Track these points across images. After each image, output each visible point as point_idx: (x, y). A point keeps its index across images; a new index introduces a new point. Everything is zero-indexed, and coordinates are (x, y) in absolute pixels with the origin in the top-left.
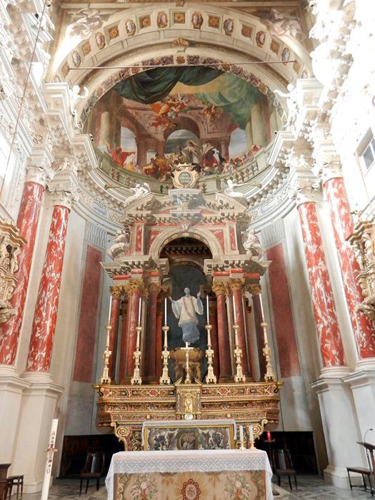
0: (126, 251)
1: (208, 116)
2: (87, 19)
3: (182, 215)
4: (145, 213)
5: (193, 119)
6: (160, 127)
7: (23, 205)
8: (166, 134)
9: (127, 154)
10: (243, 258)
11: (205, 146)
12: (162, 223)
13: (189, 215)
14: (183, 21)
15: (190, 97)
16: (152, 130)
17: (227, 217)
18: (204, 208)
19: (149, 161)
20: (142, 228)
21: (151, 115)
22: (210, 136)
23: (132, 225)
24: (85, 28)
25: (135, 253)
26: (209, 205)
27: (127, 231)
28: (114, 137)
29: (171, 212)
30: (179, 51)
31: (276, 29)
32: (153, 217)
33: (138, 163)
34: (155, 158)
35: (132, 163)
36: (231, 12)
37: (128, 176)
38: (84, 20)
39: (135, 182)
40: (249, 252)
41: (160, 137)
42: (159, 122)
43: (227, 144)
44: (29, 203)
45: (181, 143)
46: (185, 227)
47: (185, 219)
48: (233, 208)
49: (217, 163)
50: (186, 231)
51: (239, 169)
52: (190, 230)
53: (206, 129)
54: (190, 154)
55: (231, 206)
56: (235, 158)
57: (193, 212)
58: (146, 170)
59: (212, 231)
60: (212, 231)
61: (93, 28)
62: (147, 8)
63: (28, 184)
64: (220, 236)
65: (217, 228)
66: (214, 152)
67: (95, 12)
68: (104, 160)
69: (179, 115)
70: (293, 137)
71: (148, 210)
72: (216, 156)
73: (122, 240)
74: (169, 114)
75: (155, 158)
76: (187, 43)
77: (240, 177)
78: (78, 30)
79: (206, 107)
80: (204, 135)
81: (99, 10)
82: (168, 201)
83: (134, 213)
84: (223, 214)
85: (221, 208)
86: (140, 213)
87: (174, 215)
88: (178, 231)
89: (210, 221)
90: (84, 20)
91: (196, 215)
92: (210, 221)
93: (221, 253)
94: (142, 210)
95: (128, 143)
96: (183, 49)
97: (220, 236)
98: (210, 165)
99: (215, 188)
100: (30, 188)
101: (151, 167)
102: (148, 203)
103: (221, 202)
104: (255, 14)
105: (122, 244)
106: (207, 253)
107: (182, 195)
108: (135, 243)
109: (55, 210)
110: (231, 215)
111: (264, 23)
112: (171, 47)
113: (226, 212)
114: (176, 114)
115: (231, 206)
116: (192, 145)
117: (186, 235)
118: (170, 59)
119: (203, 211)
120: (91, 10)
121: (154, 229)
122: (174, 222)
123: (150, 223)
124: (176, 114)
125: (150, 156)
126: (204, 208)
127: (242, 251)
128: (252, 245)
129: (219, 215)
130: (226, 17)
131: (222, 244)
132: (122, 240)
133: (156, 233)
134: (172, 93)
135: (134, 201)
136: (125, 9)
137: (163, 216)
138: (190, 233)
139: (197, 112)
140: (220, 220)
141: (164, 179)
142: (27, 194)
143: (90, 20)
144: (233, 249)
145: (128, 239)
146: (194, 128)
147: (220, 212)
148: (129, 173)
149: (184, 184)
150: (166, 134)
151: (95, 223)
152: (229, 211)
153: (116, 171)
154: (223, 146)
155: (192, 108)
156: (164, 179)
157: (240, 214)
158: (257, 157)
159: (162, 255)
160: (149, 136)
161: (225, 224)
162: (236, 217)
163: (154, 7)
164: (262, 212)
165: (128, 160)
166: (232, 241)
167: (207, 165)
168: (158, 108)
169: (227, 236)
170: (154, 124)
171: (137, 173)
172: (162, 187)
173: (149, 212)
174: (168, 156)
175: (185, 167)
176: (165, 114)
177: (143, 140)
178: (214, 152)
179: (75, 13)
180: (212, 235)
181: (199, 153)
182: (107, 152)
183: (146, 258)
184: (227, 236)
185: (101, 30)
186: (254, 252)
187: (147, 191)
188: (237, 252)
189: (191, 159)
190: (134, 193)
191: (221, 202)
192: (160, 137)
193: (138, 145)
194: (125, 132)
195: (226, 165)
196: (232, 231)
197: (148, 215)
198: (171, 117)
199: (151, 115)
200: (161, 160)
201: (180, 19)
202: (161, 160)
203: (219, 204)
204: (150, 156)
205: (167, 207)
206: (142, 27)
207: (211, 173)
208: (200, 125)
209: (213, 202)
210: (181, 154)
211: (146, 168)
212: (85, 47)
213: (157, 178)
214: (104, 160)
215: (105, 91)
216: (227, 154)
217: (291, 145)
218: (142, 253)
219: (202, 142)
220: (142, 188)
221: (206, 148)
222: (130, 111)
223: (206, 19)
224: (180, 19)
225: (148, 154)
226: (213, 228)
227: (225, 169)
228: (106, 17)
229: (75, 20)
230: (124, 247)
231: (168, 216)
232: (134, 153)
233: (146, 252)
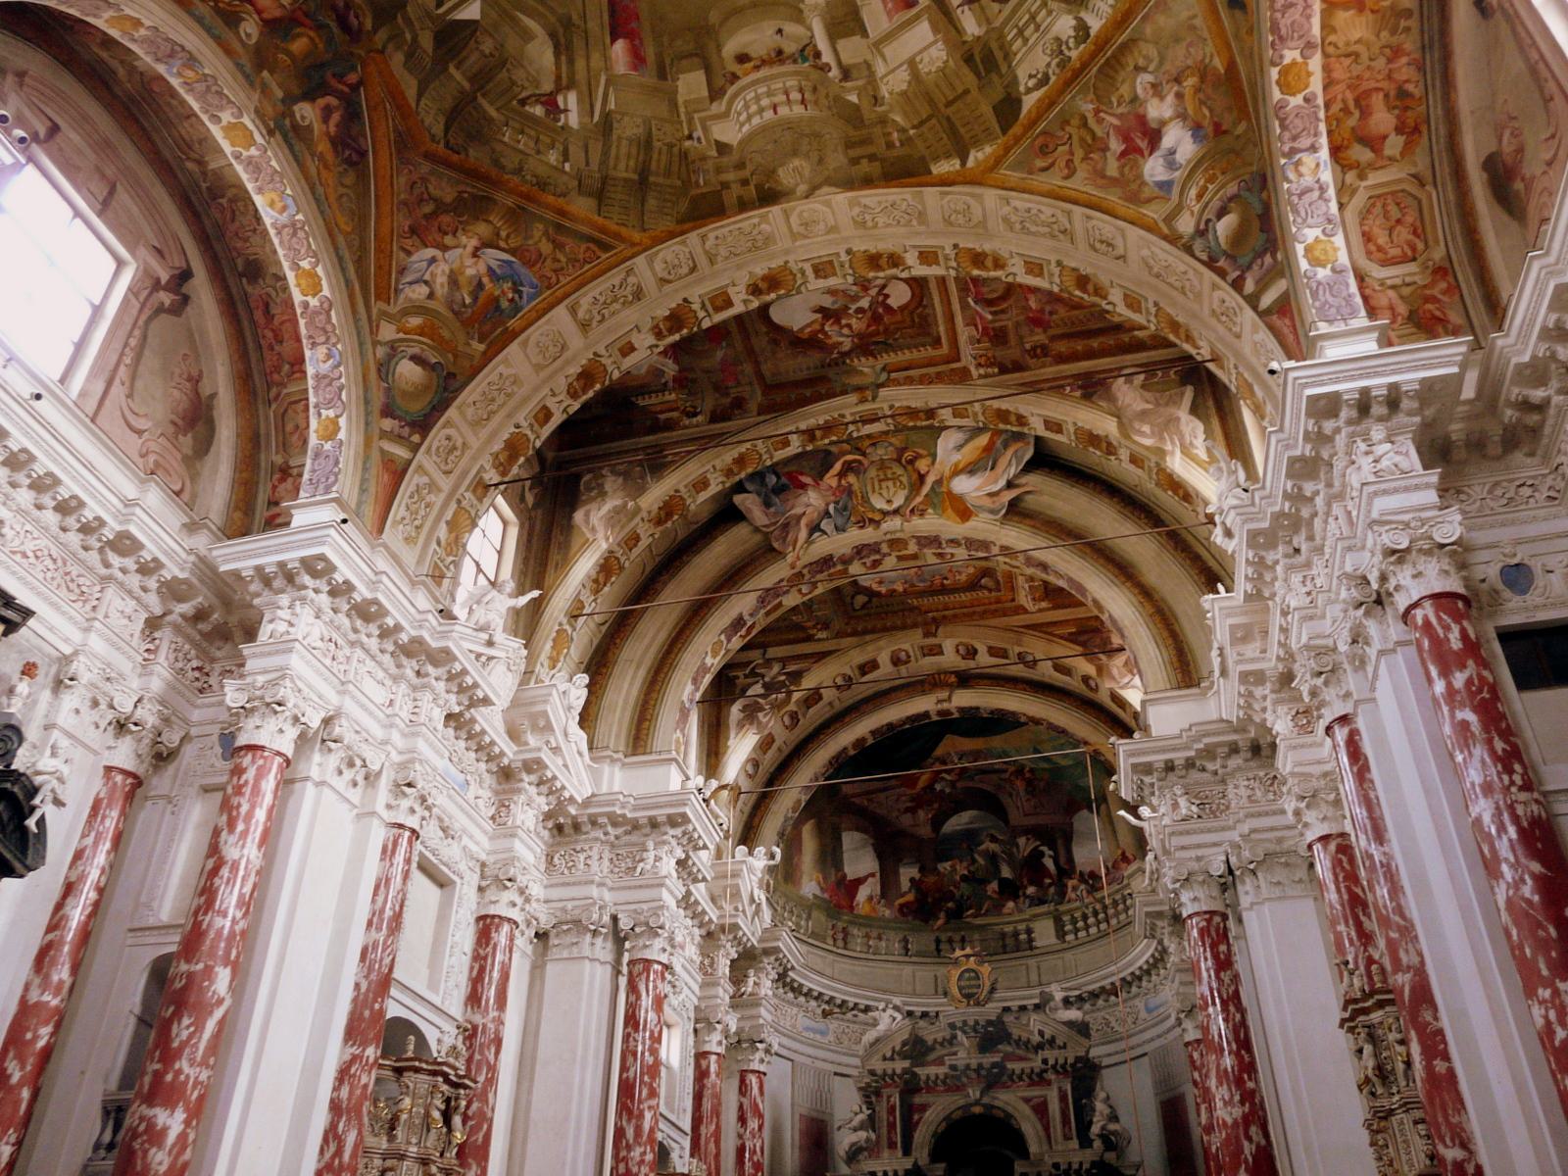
0: (870, 1149)
1: (1020, 785)
2: (765, 686)
3: (968, 1067)
4: (900, 1065)
5: (989, 789)
6: (921, 814)
7: (698, 1098)
8: (937, 823)
9: (859, 882)
10: (1087, 1157)
11: (1022, 841)
12: (931, 1087)
13: (980, 1066)
14: (941, 653)
15: (977, 755)
16: (906, 820)
17: (1054, 1067)
18: (1009, 1049)
19: (905, 885)
20: (896, 1100)
21: (900, 796)
22: (1032, 821)
23: (878, 1093)
24: (761, 709)
25: (886, 1153)
26: (1018, 1042)
27: (870, 1105)
28: (830, 856)
29: (948, 1060)
30: (939, 701)
31: (1115, 671)
32: (915, 1075)
33: (883, 895)
34: (917, 876)
35: (870, 898)
36: (1026, 639)
37: (864, 930)
38: (757, 689)
39: (880, 938)
40: (1097, 1144)
41: (925, 831)
42: (918, 802)
43: (1068, 838)
44: (707, 1093)
45: (970, 837)
46: (974, 1093)
47: (973, 1075)
48: (1065, 1047)
49: (1050, 876)
50: (977, 1103)
51: (1098, 895)
52: (985, 1100)
53: (1019, 807)
54: (993, 858)
55: (1059, 1042)
56: (1087, 870)
57: (989, 1059)
58: (902, 906)
59: (1027, 1100)
60: (1027, 1100)
61: (777, 707)
62: (870, 648)
63: (701, 1056)
64: (1041, 1109)
65: (1035, 1092)
66: (1042, 854)
67: (776, 668)
68: (815, 914)
69: (959, 785)
70: (1161, 903)
71: (905, 1058)
72: (1049, 863)
73: (861, 1127)
74: (938, 787)
75: (917, 876)
76: (953, 679)
77: (1101, 916)
78: (751, 713)
79: (1012, 769)
80: (1016, 817)
81: (784, 661)
82: (939, 1036)
83: (879, 1066)
84: (1045, 1061)
85: (1040, 1047)
86: (889, 1066)
87: (953, 1068)
88: (962, 1102)
89: (1020, 1079)
90: (757, 689)
91: (994, 1065)
92: (1020, 1079)
93: (1045, 1147)
94: (892, 1059)
95: (860, 860)
96: (944, 694)
97: (1041, 1109)
98: (1039, 884)
99: (1054, 940)
100: (704, 1063)
101: (910, 897)
102: (904, 1044)
103: (1041, 1033)
104: (1072, 638)
105: (862, 1135)
106: (1023, 1152)
107: (965, 1023)
108: (884, 1131)
109: (742, 1081)
110: (1061, 1061)
111: (1091, 661)
112: (924, 693)
113: (1051, 1055)
114: (953, 784)
115: (1059, 1042)
116: (994, 839)
117: (977, 1110)
118: (926, 715)
119: (1008, 1057)
120: (768, 663)
121: (918, 1100)
122: (953, 1083)
123: (911, 1086)
124: (953, 784)
125: (908, 873)
126: (1009, 1049)
127: (1085, 1142)
128: (1103, 1128)
129: (1037, 1064)
130: (1017, 649)
131: (1047, 1128)
132: (861, 1127)
133: (924, 1108)
134: (939, 751)
135: (877, 1040)
136: (829, 653)
137: (932, 1071)
138: (984, 1106)
139: (994, 777)
140: (1040, 1075)
141: (940, 922)
142: (701, 1075)
143: (770, 688)
144: (1067, 1138)
145: (871, 1123)
146: (991, 804)
147: (1039, 1058)
148: (867, 922)
149: (968, 996)
150: (937, 823)
151: (808, 1061)
152: (1056, 1052)
153: (840, 925)
154: (1060, 842)
155: (982, 771)
156: (940, 922)
157: (1078, 1059)
158: (1131, 876)
159: (935, 1156)
160: (902, 833)
161: (1049, 1083)
162: (1073, 1065)
163: (882, 643)
164: (1149, 1011)
165: (863, 893)
166: (1065, 1121)
167: (1031, 883)
168: (911, 781)
169: (1054, 1107)
170: (907, 810)
171: (882, 919)
172: (938, 941)
173: (906, 1064)
174: (945, 867)
175: (967, 956)
176: (930, 787)
177: (890, 847)
178: (1042, 854)
179: (740, 674)
180: (1026, 1110)
181: (1010, 855)
182: (818, 892)
183: (908, 1163)
184: (1054, 1107)
185: (792, 707)
186: (1110, 1142)
187: (899, 1017)
188: (1075, 1144)
189: (998, 870)
190: (875, 1023)
191: (1041, 1033)
192: (925, 831)
193: (881, 856)
194: (850, 839)
195: (1071, 883)
196: (1063, 1098)
197: (905, 1071)
198: (942, 791)
199: (900, 796)
200: (931, 879)
201: (936, 650)
202: (931, 879)
203: (1036, 1039)
204: (908, 873)
205: (939, 1052)
206: (864, 674)
207: (1042, 902)
208: (1005, 799)
209: (1025, 1036)
210: (974, 861)
211: (901, 901)
212: (766, 744)
213: (926, 921)
214: (815, 914)
215: (804, 798)
216: (1070, 860)
217: (1160, 915)
218: (900, 1153)
219: (1016, 832)
220: (890, 1011)
221: (1025, 845)
222: (857, 800)
223: (982, 649)
224: (936, 650)
225: (902, 870)
226: (1027, 1094)
227: (1071, 894)
228: (796, 677)
229: (744, 690)
230: (868, 1140)
231: (942, 1071)
232: (873, 875)
233: (907, 1152)
